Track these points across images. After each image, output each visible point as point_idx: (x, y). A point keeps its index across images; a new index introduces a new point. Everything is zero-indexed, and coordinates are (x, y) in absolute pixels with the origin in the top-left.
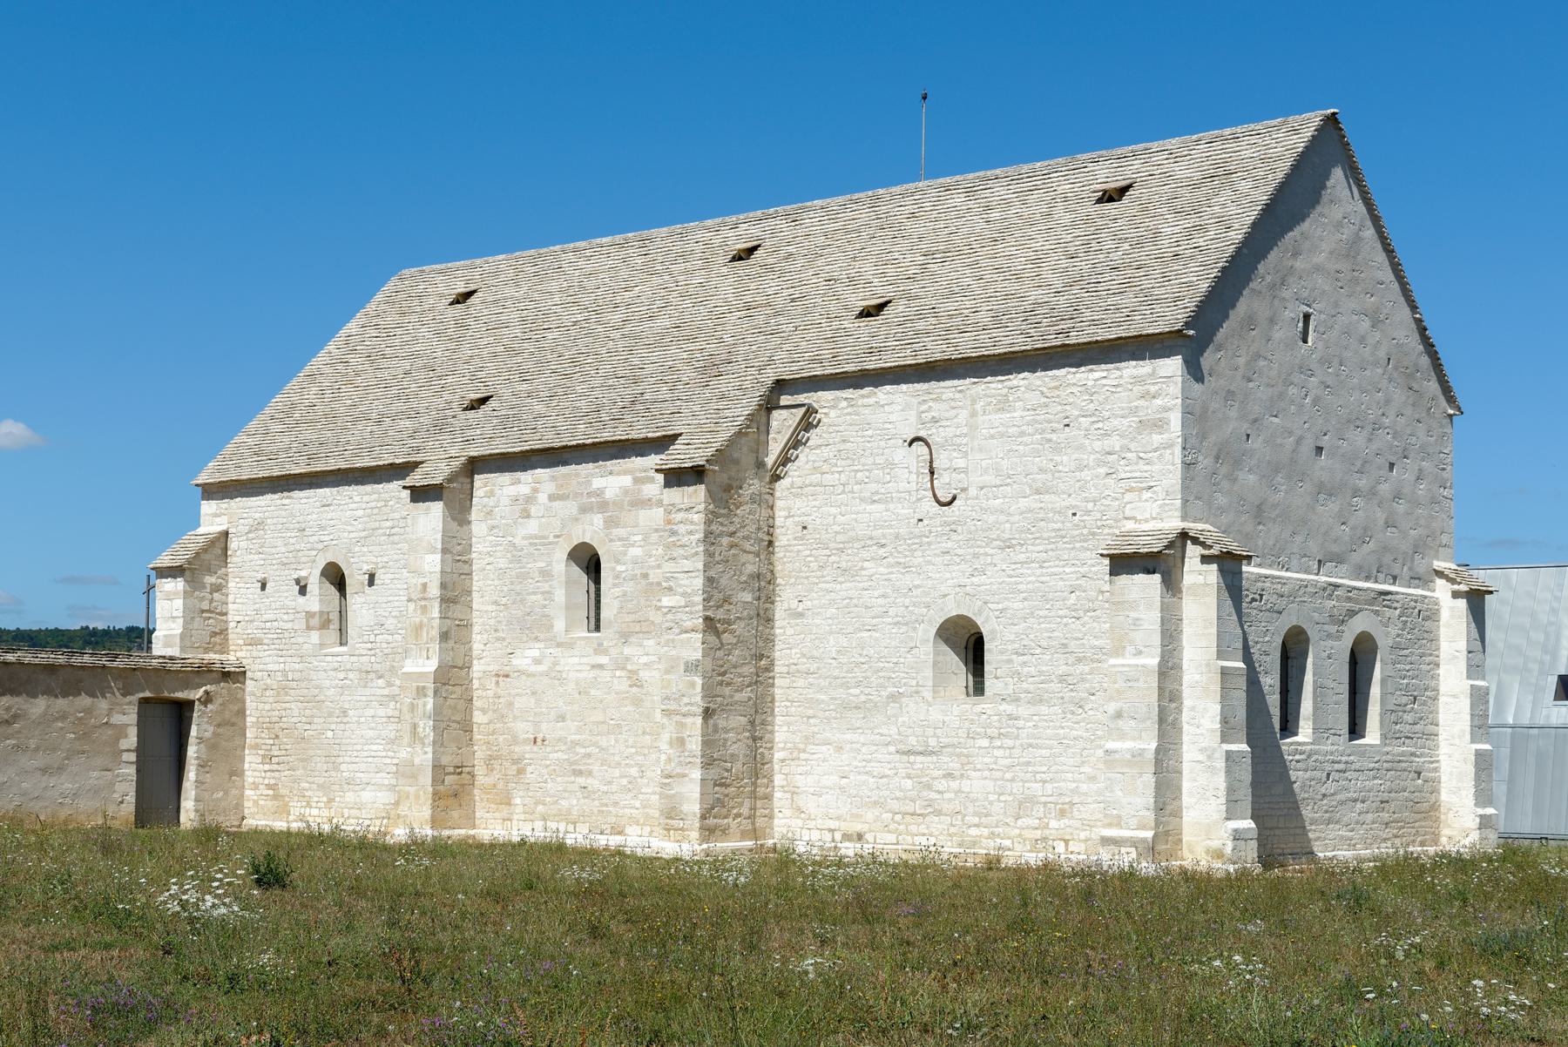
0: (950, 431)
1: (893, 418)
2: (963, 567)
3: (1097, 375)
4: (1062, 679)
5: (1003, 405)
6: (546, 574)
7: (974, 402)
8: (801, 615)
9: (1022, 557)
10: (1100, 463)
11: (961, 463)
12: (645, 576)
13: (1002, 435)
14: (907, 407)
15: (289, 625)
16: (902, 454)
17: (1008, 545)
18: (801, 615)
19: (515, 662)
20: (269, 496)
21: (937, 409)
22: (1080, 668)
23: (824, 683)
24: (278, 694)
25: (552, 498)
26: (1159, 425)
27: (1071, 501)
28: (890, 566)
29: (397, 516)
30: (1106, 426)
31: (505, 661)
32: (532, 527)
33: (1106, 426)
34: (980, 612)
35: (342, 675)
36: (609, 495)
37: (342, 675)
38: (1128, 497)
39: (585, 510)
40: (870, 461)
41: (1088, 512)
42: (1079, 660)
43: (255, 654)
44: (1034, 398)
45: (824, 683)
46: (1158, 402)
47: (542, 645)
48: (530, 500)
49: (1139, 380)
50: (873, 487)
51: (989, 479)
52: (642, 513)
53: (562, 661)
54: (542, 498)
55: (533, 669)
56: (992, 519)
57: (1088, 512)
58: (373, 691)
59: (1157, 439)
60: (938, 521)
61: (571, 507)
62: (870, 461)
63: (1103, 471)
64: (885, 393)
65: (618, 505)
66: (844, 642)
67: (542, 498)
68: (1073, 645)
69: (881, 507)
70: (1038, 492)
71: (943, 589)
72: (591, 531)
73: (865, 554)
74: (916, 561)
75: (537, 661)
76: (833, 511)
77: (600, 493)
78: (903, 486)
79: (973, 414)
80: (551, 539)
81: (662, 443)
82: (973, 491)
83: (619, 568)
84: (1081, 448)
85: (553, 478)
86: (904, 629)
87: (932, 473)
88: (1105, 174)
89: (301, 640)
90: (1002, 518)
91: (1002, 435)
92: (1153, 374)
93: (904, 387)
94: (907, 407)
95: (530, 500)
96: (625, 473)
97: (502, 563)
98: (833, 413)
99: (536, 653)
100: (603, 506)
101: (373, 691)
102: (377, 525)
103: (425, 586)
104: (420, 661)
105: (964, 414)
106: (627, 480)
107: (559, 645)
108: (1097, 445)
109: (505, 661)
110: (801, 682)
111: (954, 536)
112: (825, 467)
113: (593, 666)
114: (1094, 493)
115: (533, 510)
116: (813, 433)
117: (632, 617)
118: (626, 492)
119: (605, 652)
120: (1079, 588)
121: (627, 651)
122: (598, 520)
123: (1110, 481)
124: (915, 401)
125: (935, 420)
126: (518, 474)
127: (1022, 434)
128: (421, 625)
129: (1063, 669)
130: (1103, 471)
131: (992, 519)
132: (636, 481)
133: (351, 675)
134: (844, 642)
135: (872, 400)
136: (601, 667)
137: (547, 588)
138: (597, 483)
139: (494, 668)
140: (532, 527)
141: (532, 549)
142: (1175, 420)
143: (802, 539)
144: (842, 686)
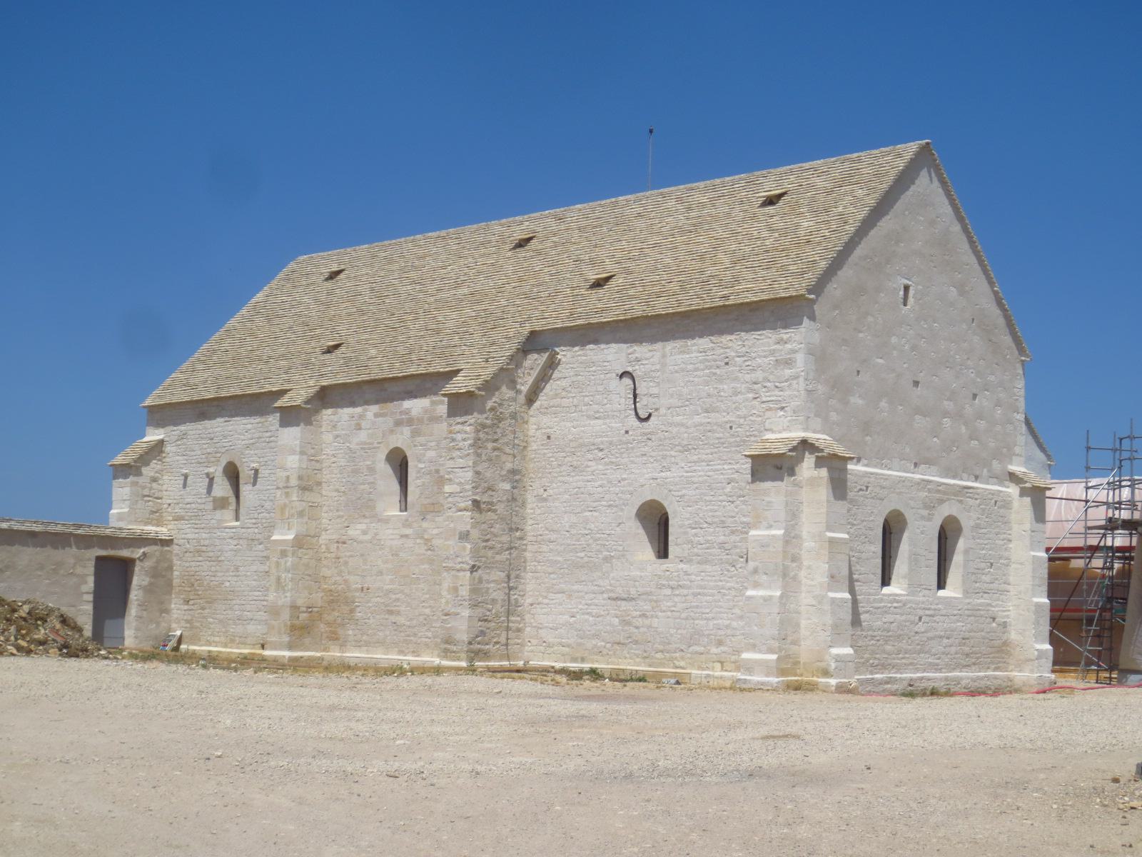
1: (609, 358)
2: (655, 464)
8: (545, 500)
9: (695, 458)
11: (655, 391)
16: (615, 383)
17: (686, 449)
18: (545, 500)
22: (733, 538)
26: (788, 363)
27: (728, 418)
28: (606, 464)
30: (753, 363)
31: (343, 532)
33: (753, 363)
35: (235, 542)
37: (235, 542)
39: (398, 423)
41: (740, 426)
42: (733, 532)
43: (180, 526)
46: (789, 346)
48: (361, 417)
51: (674, 401)
57: (740, 426)
59: (788, 372)
63: (751, 395)
65: (420, 421)
66: (574, 519)
69: (600, 422)
70: (707, 411)
72: (401, 439)
73: (590, 456)
75: (365, 533)
76: (569, 424)
77: (407, 412)
79: (664, 356)
82: (663, 411)
83: (421, 466)
84: (736, 379)
90: (683, 429)
91: (683, 370)
95: (361, 417)
99: (363, 527)
100: (410, 422)
103: (288, 477)
108: (748, 377)
109: (343, 532)
111: (649, 443)
113: (402, 536)
114: (743, 412)
115: (363, 424)
118: (426, 411)
119: (410, 526)
121: (425, 525)
122: (407, 431)
123: (755, 403)
125: (637, 360)
127: (696, 370)
128: (285, 505)
130: (751, 395)
131: (675, 430)
133: (241, 542)
134: (574, 519)
136: (406, 536)
140: (363, 436)
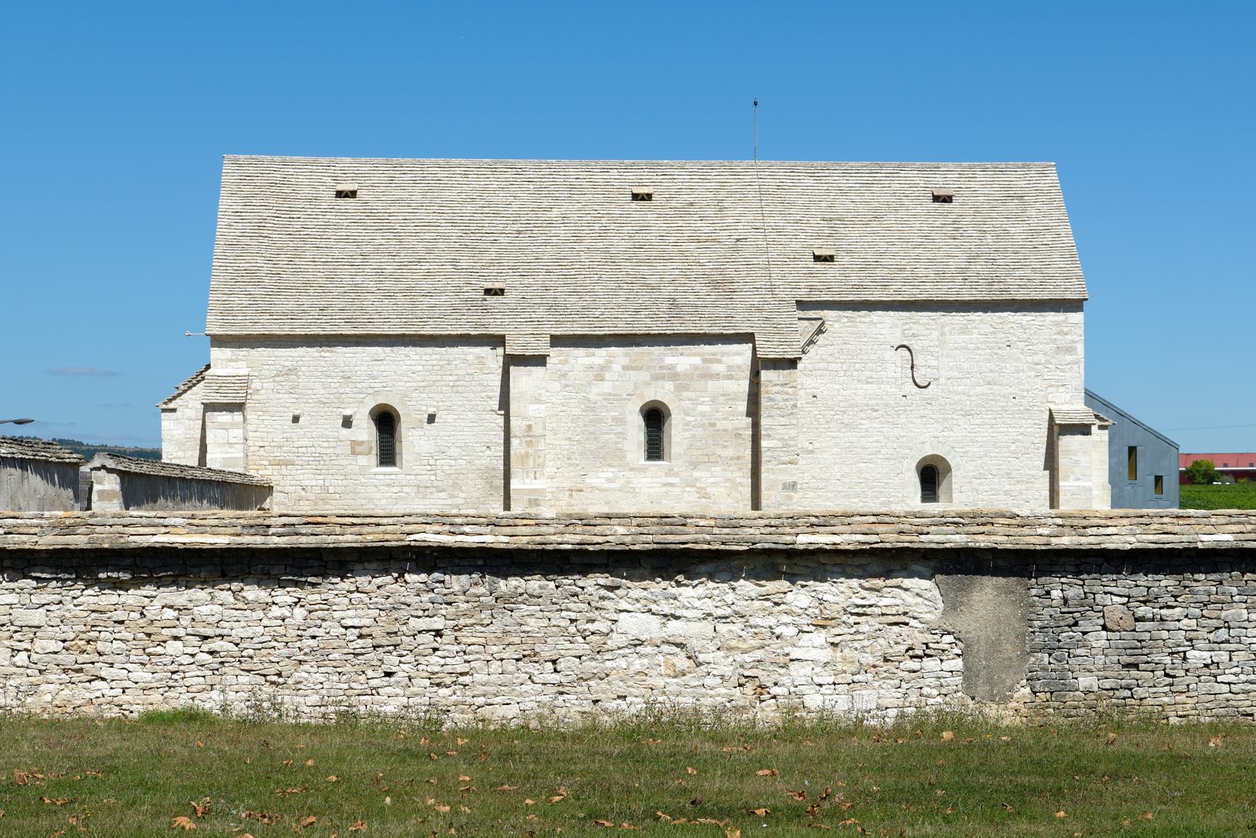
0: (926, 343)
1: (883, 332)
2: (936, 425)
3: (1029, 318)
4: (1007, 493)
5: (964, 330)
6: (620, 421)
7: (943, 327)
8: (812, 452)
9: (978, 421)
10: (1031, 369)
11: (935, 363)
12: (714, 425)
13: (963, 348)
14: (894, 326)
15: (331, 451)
16: (890, 354)
17: (967, 414)
18: (812, 452)
19: (588, 481)
20: (304, 349)
21: (916, 329)
22: (1019, 487)
23: (829, 495)
24: (316, 504)
25: (624, 368)
26: (1070, 350)
27: (1011, 390)
28: (881, 423)
29: (461, 372)
30: (1035, 348)
31: (579, 480)
32: (606, 387)
33: (1035, 348)
34: (949, 453)
35: (396, 489)
36: (680, 369)
37: (396, 489)
38: (1050, 390)
39: (656, 378)
40: (866, 357)
41: (1023, 397)
42: (1018, 482)
43: (284, 472)
44: (986, 328)
45: (829, 495)
46: (1069, 337)
47: (615, 470)
48: (604, 368)
49: (1057, 324)
50: (868, 374)
51: (955, 374)
52: (710, 383)
53: (635, 481)
54: (617, 367)
55: (607, 486)
56: (956, 398)
57: (1023, 397)
58: (432, 501)
59: (1069, 358)
60: (918, 397)
61: (645, 376)
62: (866, 357)
63: (1033, 374)
64: (877, 315)
65: (688, 376)
66: (846, 469)
67: (617, 367)
68: (1014, 474)
69: (875, 386)
70: (989, 383)
71: (922, 439)
72: (662, 393)
73: (863, 415)
74: (902, 421)
75: (609, 480)
76: (837, 386)
77: (672, 367)
78: (891, 374)
79: (943, 334)
80: (624, 396)
81: (748, 338)
82: (942, 381)
83: (688, 419)
84: (1018, 360)
85: (627, 355)
86: (892, 462)
87: (912, 368)
88: (941, 184)
89: (343, 462)
90: (964, 397)
91: (963, 348)
92: (1065, 321)
93: (891, 313)
94: (894, 326)
95: (604, 368)
96: (695, 355)
97: (576, 411)
98: (836, 325)
99: (610, 475)
100: (674, 376)
101: (432, 501)
102: (439, 378)
103: (530, 427)
104: (528, 481)
105: (936, 334)
106: (697, 360)
107: (631, 470)
108: (1029, 359)
109: (579, 480)
110: (812, 494)
111: (929, 407)
112: (830, 359)
113: (665, 485)
114: (1027, 387)
115: (607, 376)
116: (821, 337)
117: (699, 452)
118: (696, 368)
119: (676, 475)
120: (1018, 441)
121: (696, 474)
122: (669, 386)
123: (1038, 380)
124: (900, 322)
125: (914, 335)
126: (593, 350)
127: (978, 348)
128: (527, 455)
129: (1007, 487)
130: (1033, 374)
131: (956, 398)
132: (705, 361)
133: (406, 489)
134: (846, 469)
135: (868, 319)
136: (672, 485)
137: (620, 430)
138: (669, 360)
139: (567, 485)
140: (606, 387)
141: (605, 403)
142: (1080, 348)
143: (813, 403)
144: (844, 497)
